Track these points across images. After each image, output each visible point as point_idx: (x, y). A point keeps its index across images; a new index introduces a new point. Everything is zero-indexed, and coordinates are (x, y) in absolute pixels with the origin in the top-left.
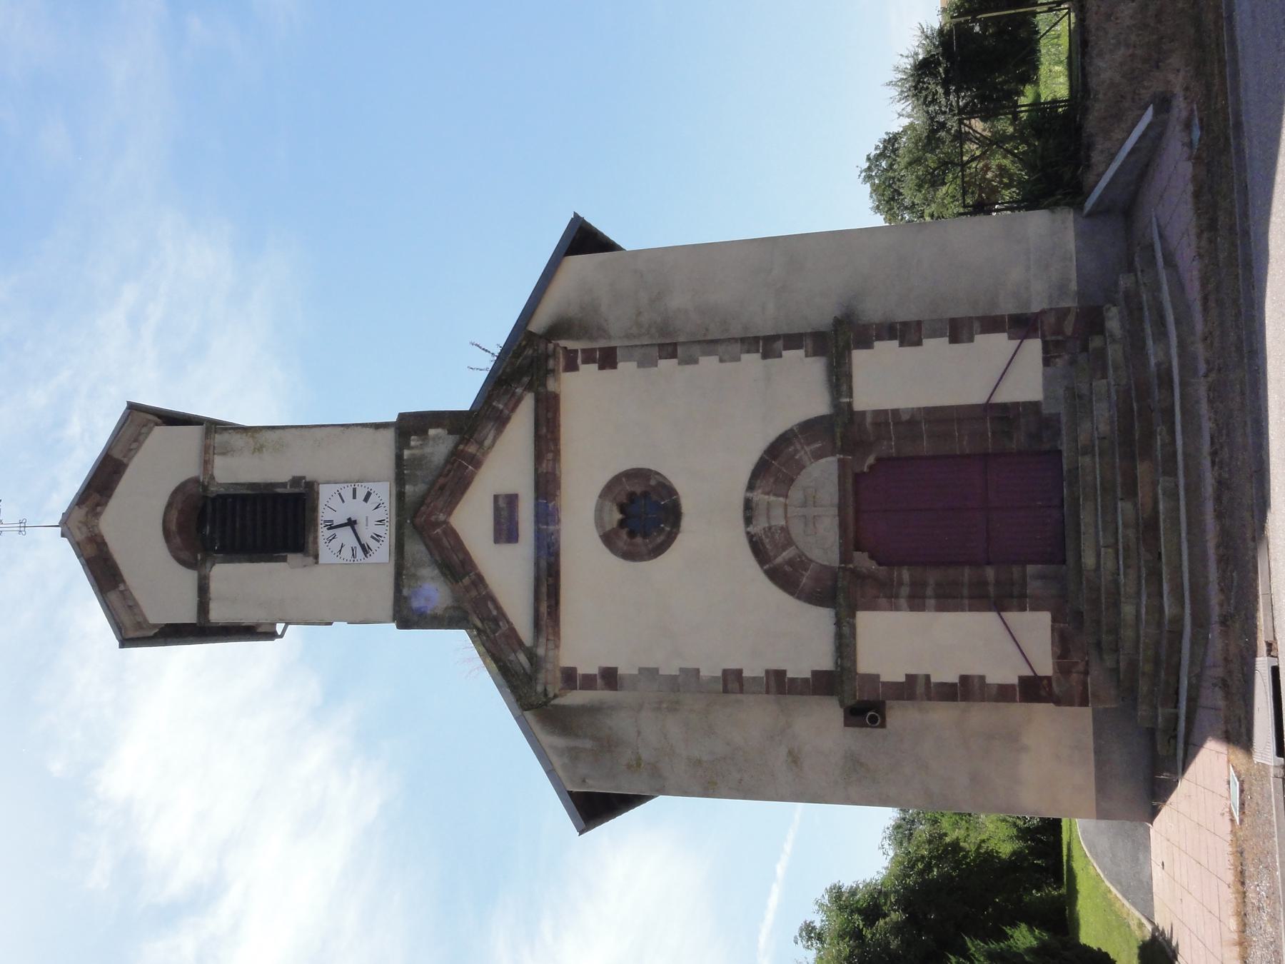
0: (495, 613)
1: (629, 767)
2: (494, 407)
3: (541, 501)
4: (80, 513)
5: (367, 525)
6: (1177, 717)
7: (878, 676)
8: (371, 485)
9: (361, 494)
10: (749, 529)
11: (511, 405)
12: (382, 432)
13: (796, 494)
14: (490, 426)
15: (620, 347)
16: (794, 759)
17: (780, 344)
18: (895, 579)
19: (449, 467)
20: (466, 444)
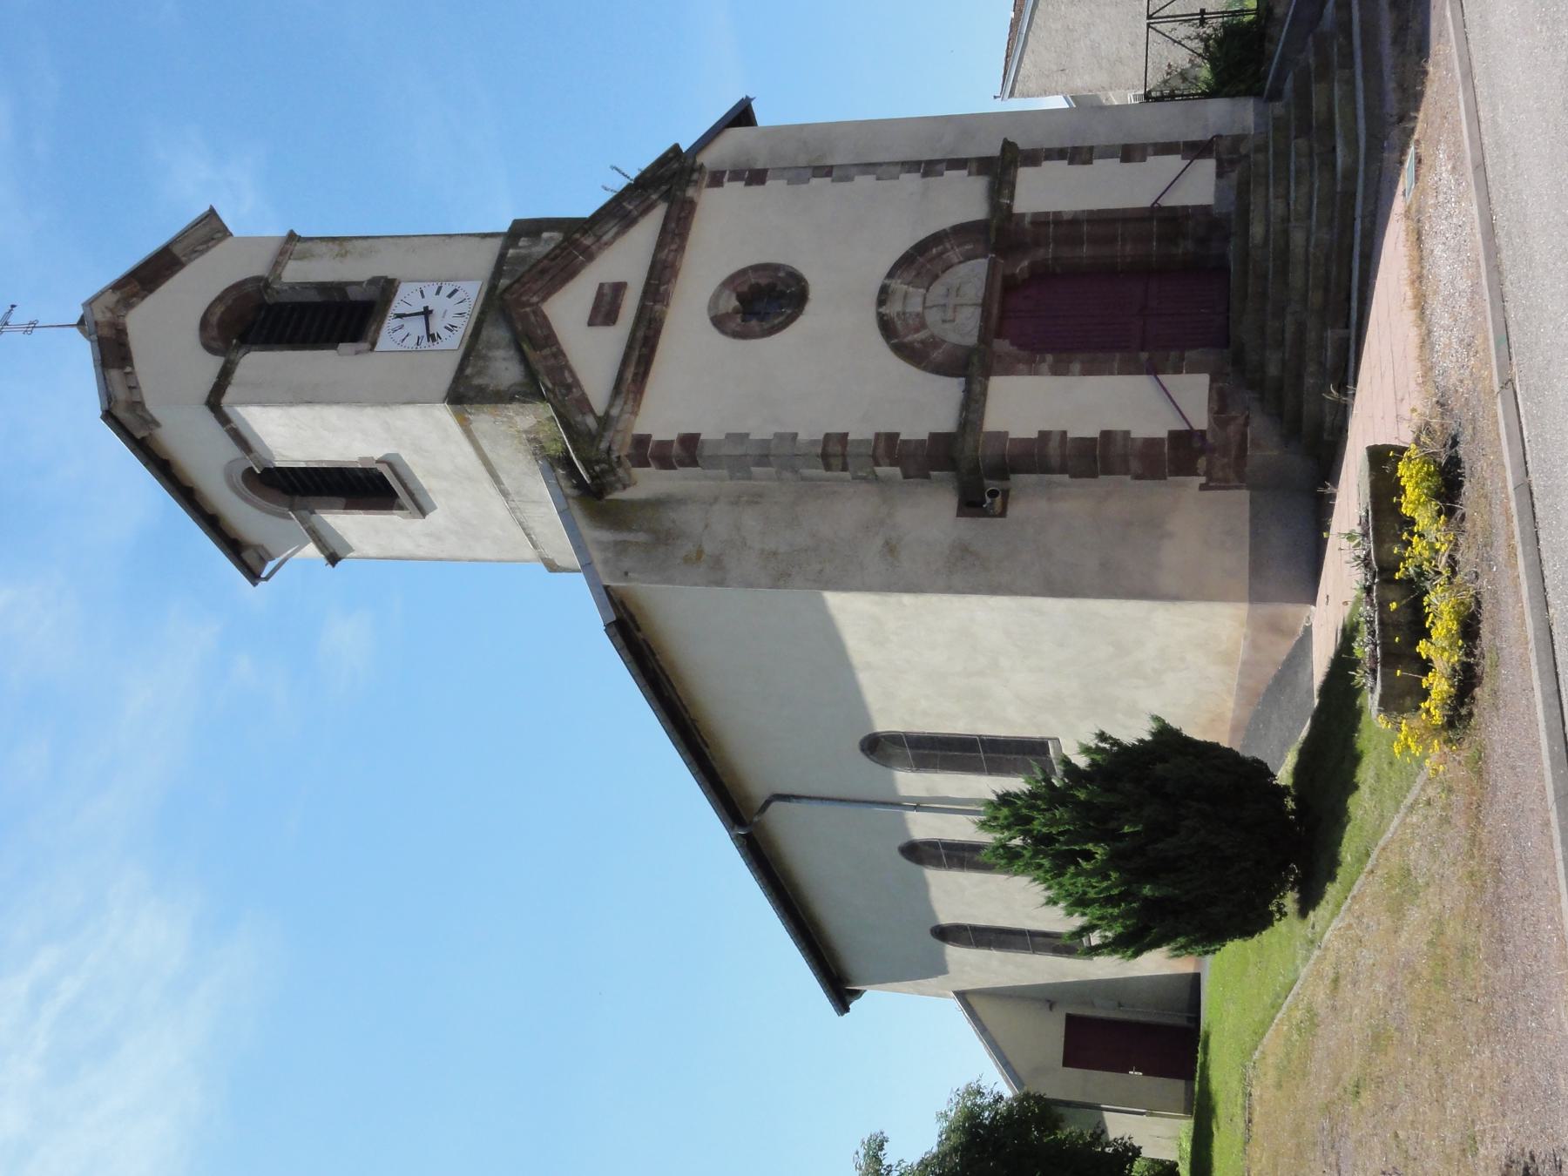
0: (570, 380)
1: (686, 560)
2: (624, 207)
3: (652, 282)
4: (112, 298)
5: (443, 317)
6: (1348, 339)
7: (1006, 433)
8: (457, 284)
9: (447, 289)
10: (881, 310)
11: (641, 209)
12: (489, 241)
13: (938, 289)
14: (611, 224)
15: (773, 169)
16: (891, 549)
17: (939, 167)
18: (1051, 235)
19: (558, 251)
20: (583, 235)
